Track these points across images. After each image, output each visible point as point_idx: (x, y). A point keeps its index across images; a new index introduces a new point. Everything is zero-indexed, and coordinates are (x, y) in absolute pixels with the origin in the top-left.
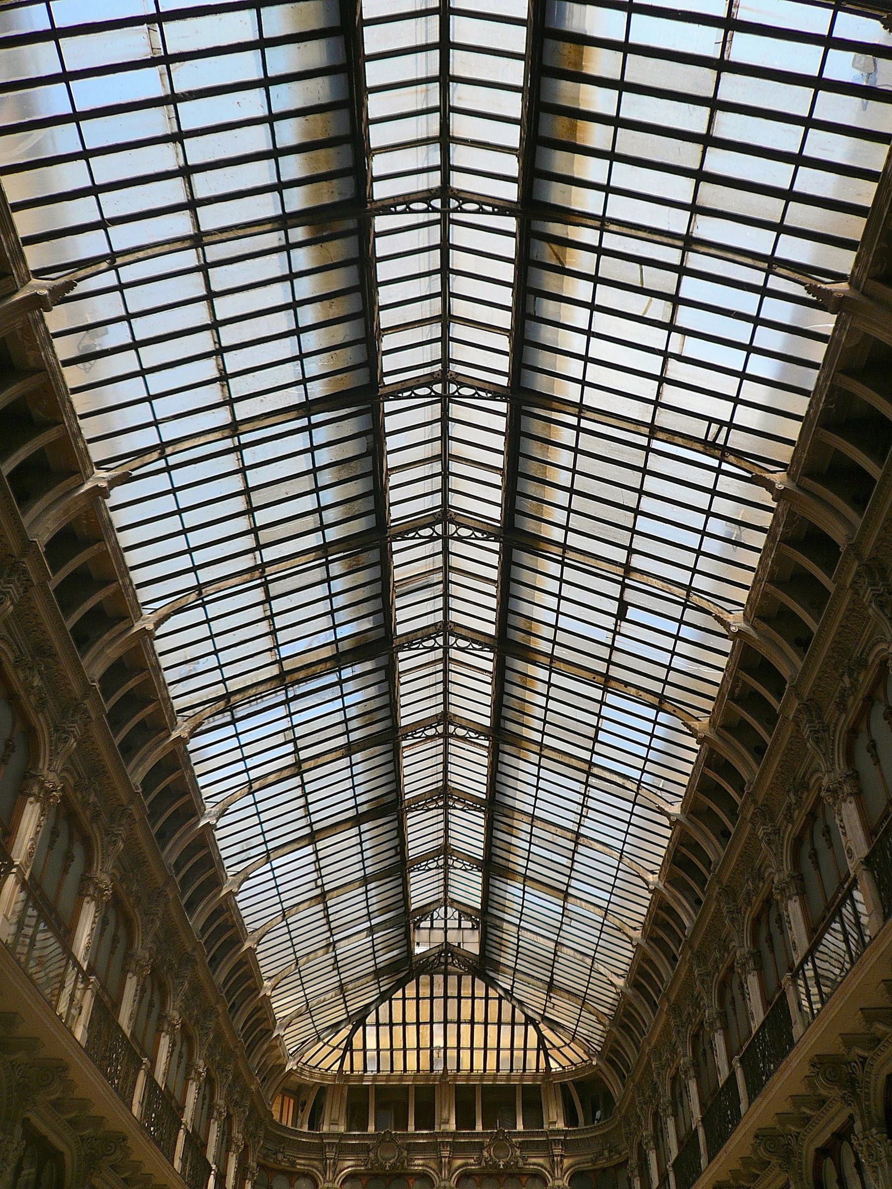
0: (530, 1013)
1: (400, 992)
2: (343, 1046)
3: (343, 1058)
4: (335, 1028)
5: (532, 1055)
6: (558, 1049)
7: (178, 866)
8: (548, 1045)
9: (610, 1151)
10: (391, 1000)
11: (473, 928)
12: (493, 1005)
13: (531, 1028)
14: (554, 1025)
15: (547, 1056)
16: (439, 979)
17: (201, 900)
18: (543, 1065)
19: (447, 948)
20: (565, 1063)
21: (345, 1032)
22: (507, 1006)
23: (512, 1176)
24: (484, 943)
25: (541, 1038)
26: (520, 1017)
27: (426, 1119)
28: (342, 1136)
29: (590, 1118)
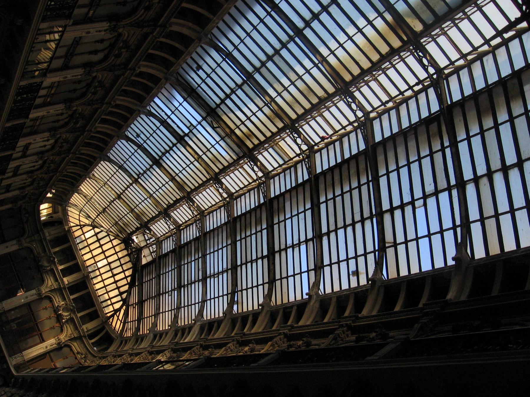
0: (128, 299)
1: (113, 238)
2: (82, 223)
3: (77, 225)
4: (88, 217)
5: (111, 308)
6: (118, 319)
7: (117, 106)
8: (118, 314)
9: (84, 357)
10: (108, 235)
12: (124, 282)
13: (121, 303)
14: (126, 314)
15: (113, 316)
16: (125, 252)
17: (109, 125)
18: (109, 315)
19: (139, 250)
20: (114, 324)
21: (87, 222)
22: (126, 288)
24: (148, 264)
25: (119, 310)
27: (66, 272)
28: (45, 239)
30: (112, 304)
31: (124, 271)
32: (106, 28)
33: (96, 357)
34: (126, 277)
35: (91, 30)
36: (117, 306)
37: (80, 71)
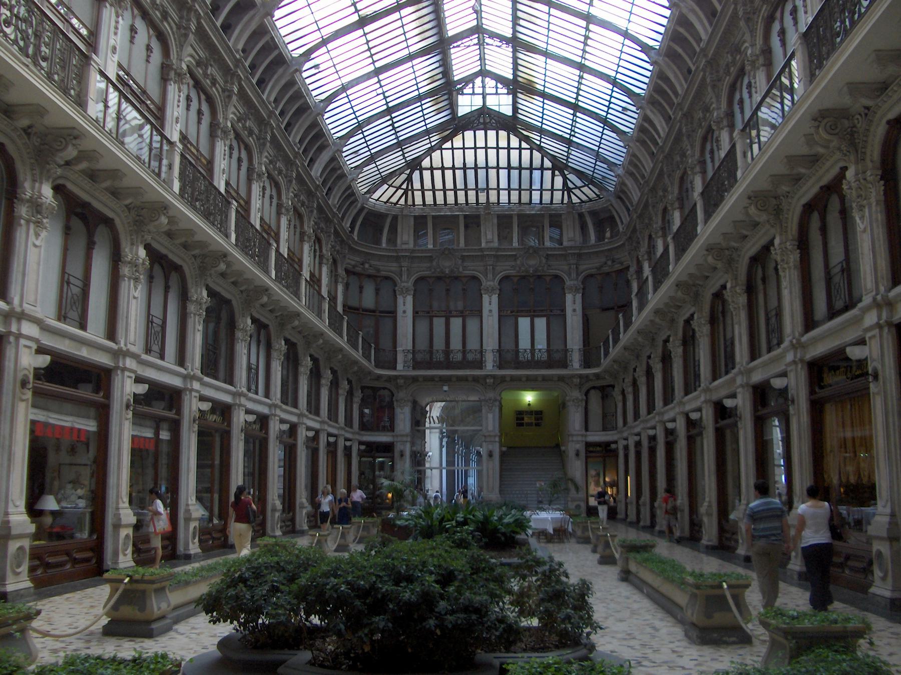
2: (404, 186)
6: (576, 187)
8: (570, 185)
11: (508, 94)
23: (539, 277)
25: (565, 179)
26: (548, 163)
29: (600, 237)
30: (552, 190)
31: (509, 148)
32: (114, 15)
33: (623, 245)
34: (520, 149)
35: (112, 42)
36: (559, 181)
37: (172, 88)
